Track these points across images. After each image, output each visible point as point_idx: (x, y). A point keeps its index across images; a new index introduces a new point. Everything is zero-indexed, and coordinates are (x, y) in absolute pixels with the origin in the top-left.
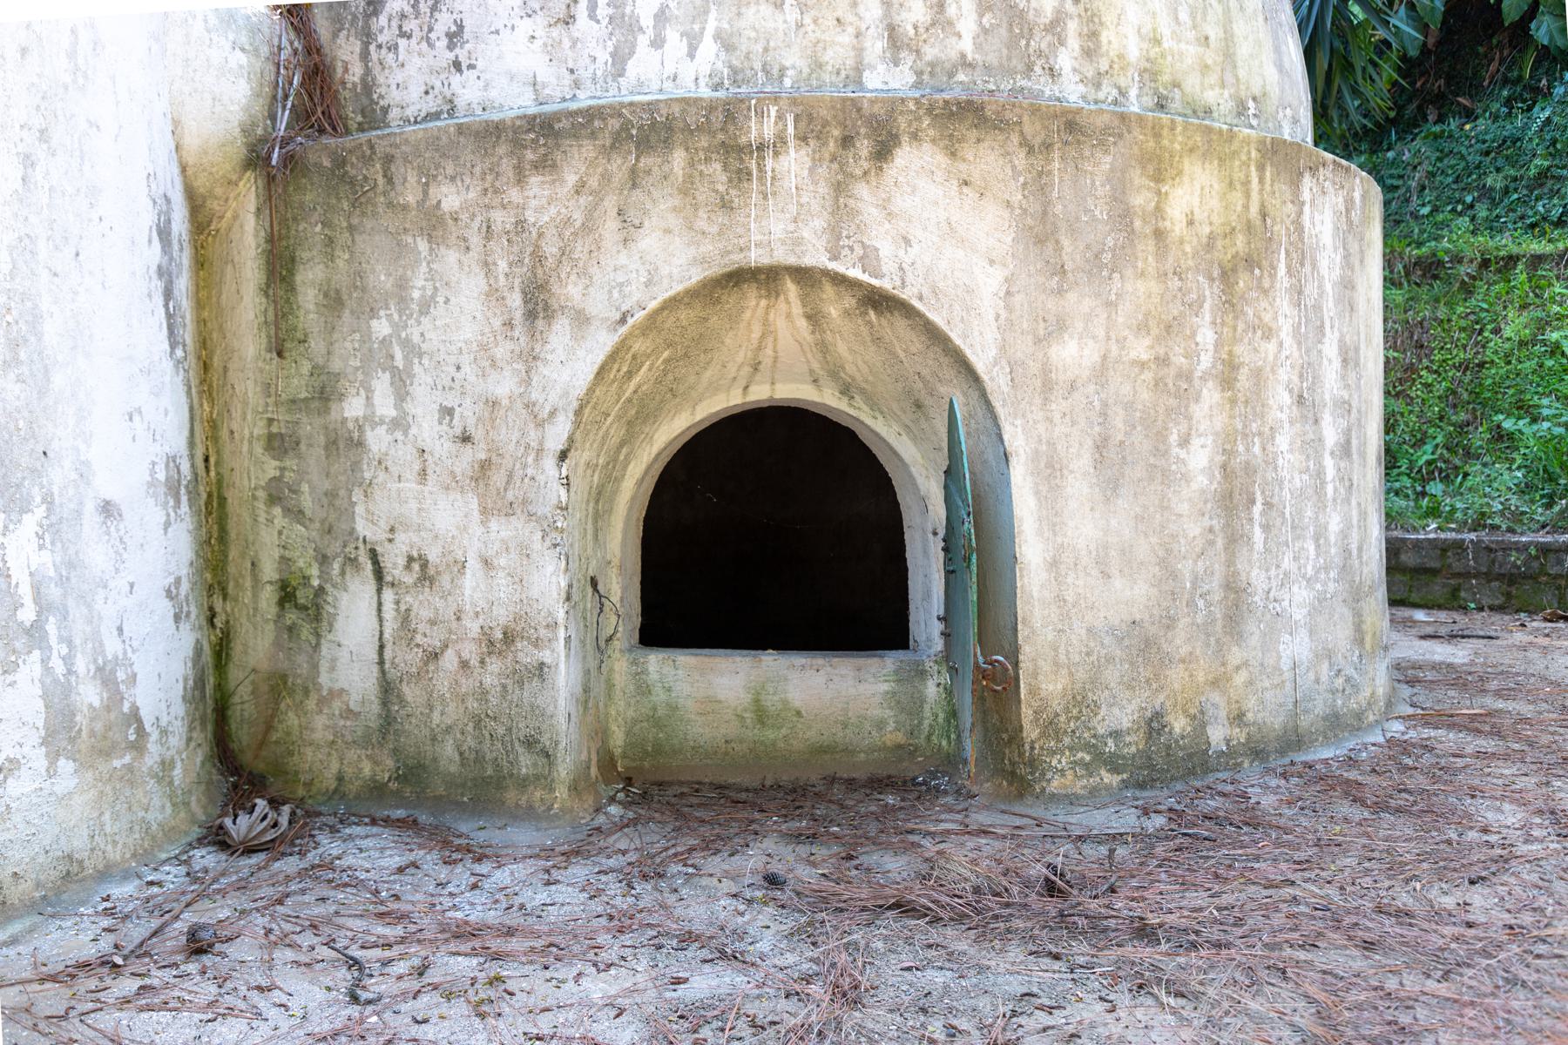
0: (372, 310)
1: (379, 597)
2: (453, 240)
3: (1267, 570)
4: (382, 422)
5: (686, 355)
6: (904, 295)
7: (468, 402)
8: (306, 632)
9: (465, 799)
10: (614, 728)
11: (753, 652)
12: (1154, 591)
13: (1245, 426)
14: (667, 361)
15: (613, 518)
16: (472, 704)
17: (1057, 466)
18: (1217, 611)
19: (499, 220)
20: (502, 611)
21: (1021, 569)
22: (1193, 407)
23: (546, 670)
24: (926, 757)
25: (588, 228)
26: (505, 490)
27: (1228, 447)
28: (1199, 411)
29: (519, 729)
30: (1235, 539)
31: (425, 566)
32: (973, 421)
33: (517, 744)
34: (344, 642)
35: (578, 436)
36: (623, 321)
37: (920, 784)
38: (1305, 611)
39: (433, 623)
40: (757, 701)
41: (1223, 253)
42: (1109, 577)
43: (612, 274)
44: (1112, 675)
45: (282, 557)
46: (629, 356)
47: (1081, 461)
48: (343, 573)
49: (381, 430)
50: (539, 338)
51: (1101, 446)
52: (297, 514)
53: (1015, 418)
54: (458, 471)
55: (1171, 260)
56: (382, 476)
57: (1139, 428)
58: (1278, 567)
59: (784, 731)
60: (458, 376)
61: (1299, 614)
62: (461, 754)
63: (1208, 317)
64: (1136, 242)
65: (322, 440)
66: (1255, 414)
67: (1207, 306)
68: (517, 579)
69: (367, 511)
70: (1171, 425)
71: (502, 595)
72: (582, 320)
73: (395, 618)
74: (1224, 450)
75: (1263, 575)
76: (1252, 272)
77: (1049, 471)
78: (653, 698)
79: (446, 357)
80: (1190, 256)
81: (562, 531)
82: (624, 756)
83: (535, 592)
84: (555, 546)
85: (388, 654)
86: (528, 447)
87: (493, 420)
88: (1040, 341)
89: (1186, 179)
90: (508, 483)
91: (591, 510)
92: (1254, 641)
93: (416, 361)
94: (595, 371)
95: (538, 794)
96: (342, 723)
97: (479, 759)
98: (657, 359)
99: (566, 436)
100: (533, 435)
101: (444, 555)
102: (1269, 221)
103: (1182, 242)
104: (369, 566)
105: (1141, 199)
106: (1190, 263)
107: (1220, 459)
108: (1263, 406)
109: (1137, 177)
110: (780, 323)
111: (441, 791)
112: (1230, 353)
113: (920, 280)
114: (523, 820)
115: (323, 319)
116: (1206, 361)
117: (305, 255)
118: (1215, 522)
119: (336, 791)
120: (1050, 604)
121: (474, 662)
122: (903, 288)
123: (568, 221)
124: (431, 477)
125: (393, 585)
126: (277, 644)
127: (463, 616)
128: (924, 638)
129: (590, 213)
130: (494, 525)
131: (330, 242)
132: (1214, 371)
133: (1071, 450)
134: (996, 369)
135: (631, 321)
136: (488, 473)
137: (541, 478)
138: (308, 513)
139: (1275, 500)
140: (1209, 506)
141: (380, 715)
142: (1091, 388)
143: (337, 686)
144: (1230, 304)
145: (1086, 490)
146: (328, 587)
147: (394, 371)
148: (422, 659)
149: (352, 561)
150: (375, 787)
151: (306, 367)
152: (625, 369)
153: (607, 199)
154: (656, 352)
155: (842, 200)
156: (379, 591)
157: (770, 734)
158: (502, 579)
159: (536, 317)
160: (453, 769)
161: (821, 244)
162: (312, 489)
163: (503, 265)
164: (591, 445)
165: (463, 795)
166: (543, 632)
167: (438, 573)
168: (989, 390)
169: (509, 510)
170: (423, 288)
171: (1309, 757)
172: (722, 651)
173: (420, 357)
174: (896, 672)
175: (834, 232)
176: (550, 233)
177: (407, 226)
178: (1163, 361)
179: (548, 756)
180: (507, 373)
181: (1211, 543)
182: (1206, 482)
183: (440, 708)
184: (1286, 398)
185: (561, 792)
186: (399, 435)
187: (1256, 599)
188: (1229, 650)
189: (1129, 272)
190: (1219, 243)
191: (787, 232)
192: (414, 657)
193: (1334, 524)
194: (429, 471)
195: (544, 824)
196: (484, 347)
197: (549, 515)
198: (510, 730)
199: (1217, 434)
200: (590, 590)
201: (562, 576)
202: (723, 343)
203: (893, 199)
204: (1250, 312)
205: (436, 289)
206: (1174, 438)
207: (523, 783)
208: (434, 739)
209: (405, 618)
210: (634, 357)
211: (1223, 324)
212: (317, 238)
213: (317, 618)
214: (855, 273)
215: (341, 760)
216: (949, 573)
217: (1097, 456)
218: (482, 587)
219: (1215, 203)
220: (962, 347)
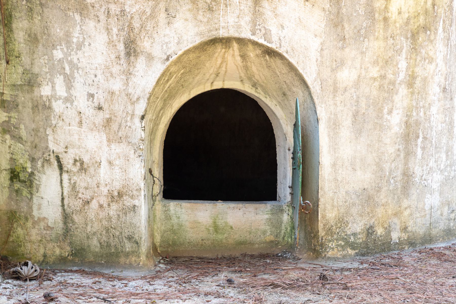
0: (53, 45)
1: (61, 177)
2: (92, 15)
3: (422, 167)
4: (60, 98)
5: (190, 71)
6: (281, 51)
7: (100, 91)
8: (25, 192)
9: (103, 262)
10: (156, 234)
11: (212, 202)
12: (373, 176)
13: (417, 104)
14: (182, 74)
15: (155, 142)
16: (105, 223)
17: (337, 124)
18: (399, 184)
19: (113, 9)
20: (117, 184)
21: (321, 167)
23: (136, 208)
24: (282, 246)
25: (153, 16)
26: (118, 131)
27: (409, 113)
28: (397, 98)
29: (125, 233)
30: (409, 154)
31: (82, 163)
32: (306, 104)
33: (124, 239)
34: (44, 196)
35: (148, 109)
36: (168, 59)
37: (280, 256)
38: (439, 184)
39: (86, 188)
40: (215, 223)
41: (413, 26)
42: (356, 170)
43: (163, 38)
45: (11, 158)
46: (168, 74)
48: (43, 166)
49: (60, 102)
50: (132, 65)
51: (355, 115)
52: (19, 139)
53: (322, 104)
54: (97, 122)
55: (390, 31)
56: (61, 123)
57: (371, 107)
58: (427, 165)
59: (225, 235)
60: (96, 80)
61: (435, 186)
62: (100, 243)
63: (404, 56)
64: (375, 24)
65: (30, 105)
67: (404, 51)
68: (123, 170)
69: (54, 139)
70: (385, 105)
71: (117, 177)
72: (150, 58)
73: (69, 186)
74: (407, 115)
75: (420, 169)
76: (426, 33)
77: (334, 126)
78: (172, 221)
79: (90, 71)
80: (398, 28)
81: (142, 150)
82: (160, 246)
83: (131, 176)
84: (140, 156)
85: (66, 202)
86: (127, 113)
87: (112, 101)
88: (333, 70)
90: (119, 128)
91: (149, 139)
93: (76, 71)
94: (156, 81)
95: (133, 259)
96: (45, 232)
97: (109, 245)
98: (179, 73)
99: (144, 109)
100: (130, 108)
101: (91, 159)
102: (436, 7)
104: (56, 163)
107: (405, 119)
110: (229, 58)
111: (92, 259)
113: (287, 44)
114: (129, 269)
115: (28, 47)
116: (402, 76)
117: (18, 15)
118: (400, 147)
119: (43, 261)
120: (331, 181)
121: (105, 205)
122: (280, 48)
123: (144, 12)
124: (84, 125)
125: (67, 172)
126: (10, 198)
127: (100, 186)
128: (283, 195)
129: (153, 9)
130: (113, 146)
131: (31, 10)
132: (405, 80)
133: (343, 117)
134: (316, 82)
135: (171, 60)
136: (110, 124)
137: (133, 127)
138: (24, 138)
139: (428, 136)
140: (399, 139)
141: (63, 228)
142: (353, 90)
143: (42, 216)
144: (415, 49)
146: (36, 172)
147: (65, 75)
148: (82, 204)
149: (48, 161)
150: (62, 259)
151: (20, 70)
152: (166, 79)
153: (161, 3)
154: (178, 71)
155: (257, 8)
156: (61, 174)
157: (220, 237)
158: (117, 170)
159: (130, 56)
160: (97, 250)
161: (248, 28)
162: (26, 128)
163: (115, 30)
164: (152, 111)
165: (101, 260)
166: (135, 193)
167: (88, 167)
168: (312, 92)
169: (120, 140)
170: (78, 37)
171: (432, 246)
172: (199, 201)
173: (78, 69)
174: (271, 210)
175: (254, 23)
176: (136, 17)
177: (70, 7)
178: (383, 77)
179: (137, 243)
180: (118, 80)
181: (399, 156)
183: (90, 225)
184: (437, 90)
185: (143, 258)
186: (68, 105)
187: (416, 179)
189: (372, 38)
190: (412, 22)
191: (235, 22)
192: (78, 204)
194: (84, 122)
195: (138, 270)
196: (107, 67)
197: (137, 143)
198: (121, 233)
200: (149, 174)
201: (143, 169)
202: (205, 66)
203: (277, 8)
204: (423, 51)
205: (84, 38)
206: (385, 111)
207: (127, 255)
208: (88, 238)
209: (74, 187)
210: (170, 74)
212: (23, 7)
213: (31, 186)
214: (261, 41)
215: (45, 248)
216: (294, 169)
217: (354, 119)
218: (108, 173)
220: (303, 73)
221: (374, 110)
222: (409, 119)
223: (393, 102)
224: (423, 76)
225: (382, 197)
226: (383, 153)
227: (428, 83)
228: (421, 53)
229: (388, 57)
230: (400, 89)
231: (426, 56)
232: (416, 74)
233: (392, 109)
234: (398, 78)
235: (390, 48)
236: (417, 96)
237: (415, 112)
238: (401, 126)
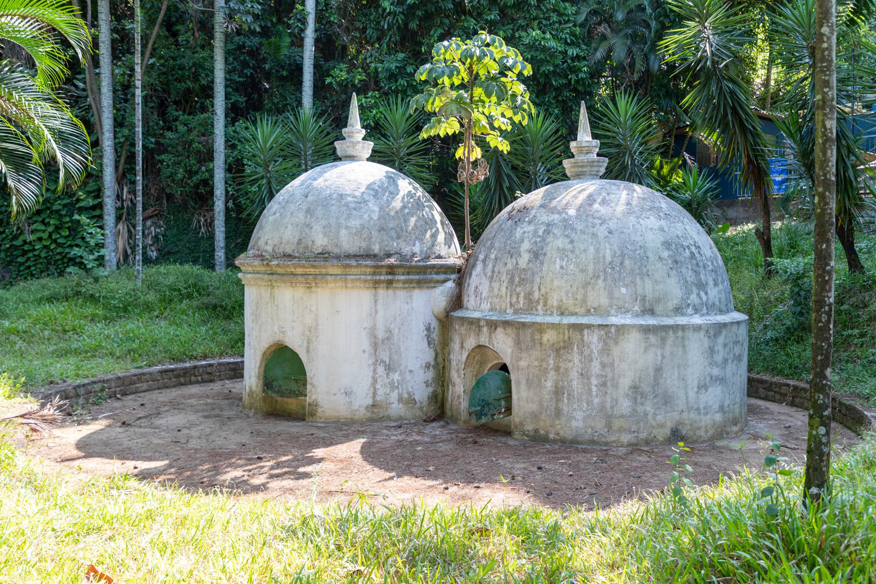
30: (558, 400)
44: (528, 420)
47: (524, 382)
51: (528, 380)
92: (564, 420)
109: (536, 333)
116: (551, 366)
178: (541, 366)
193: (596, 401)
225: (543, 417)
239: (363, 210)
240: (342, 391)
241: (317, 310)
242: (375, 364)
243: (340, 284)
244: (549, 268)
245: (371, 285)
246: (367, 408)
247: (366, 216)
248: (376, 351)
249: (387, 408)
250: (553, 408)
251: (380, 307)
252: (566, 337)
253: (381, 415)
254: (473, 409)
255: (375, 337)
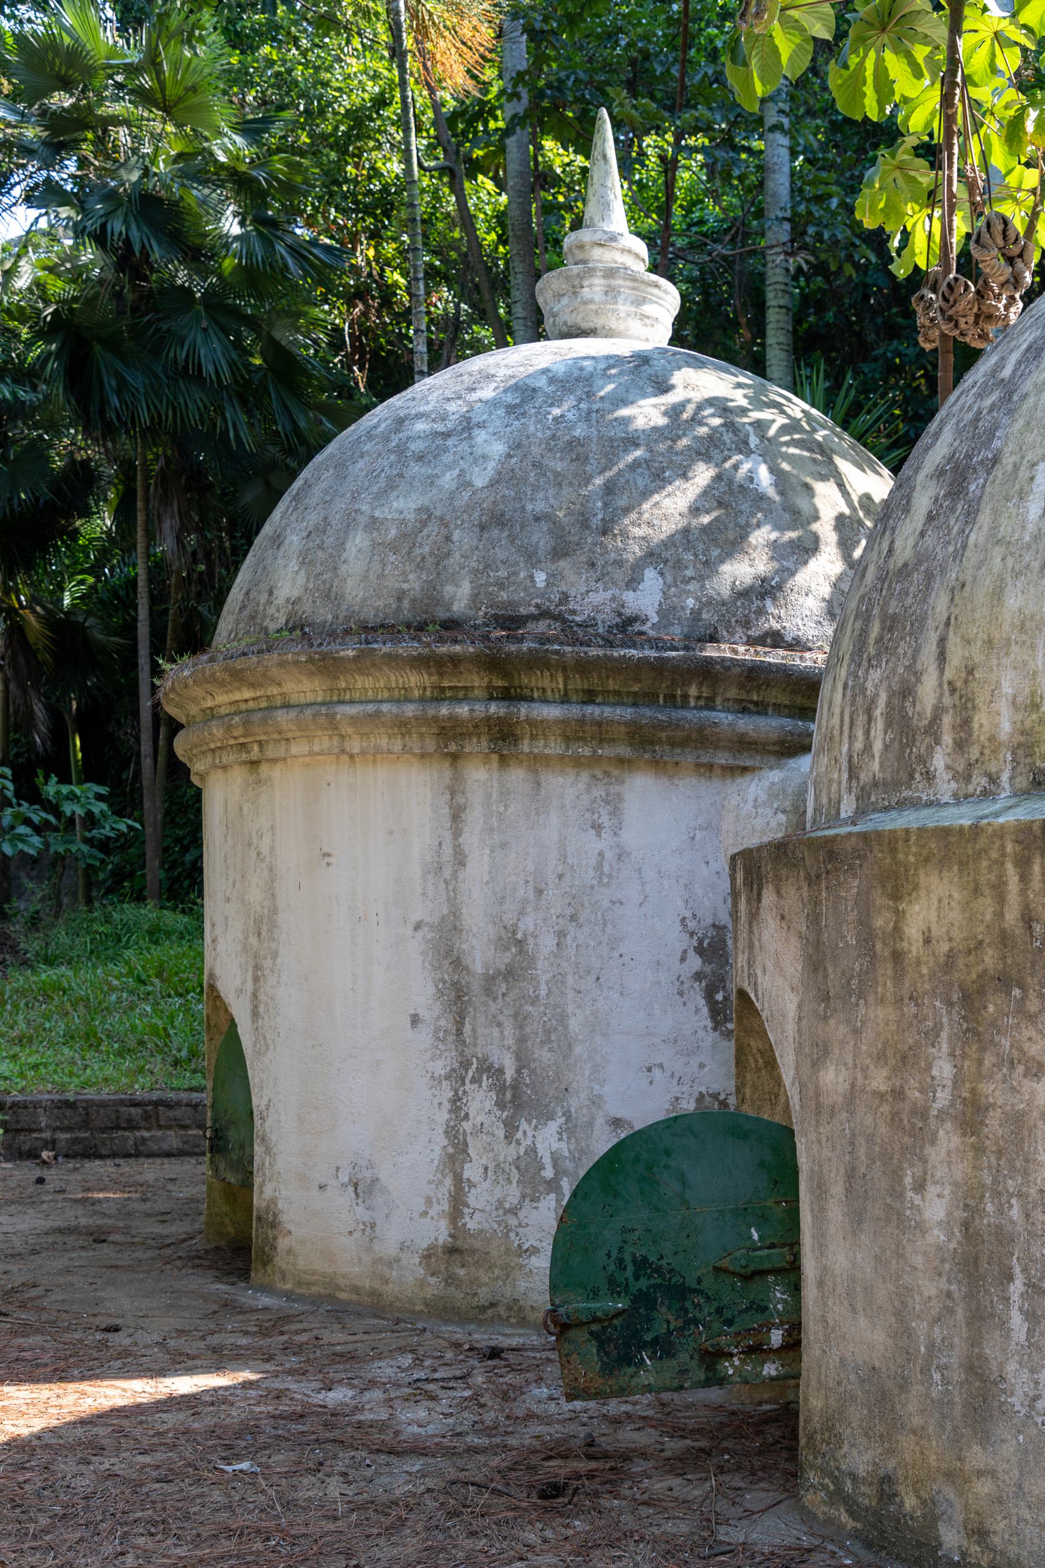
13: (996, 1181)
18: (956, 1393)
22: (929, 1150)
27: (972, 1203)
28: (936, 1154)
44: (856, 1414)
47: (837, 1189)
63: (945, 1048)
66: (1013, 1169)
67: (944, 1035)
74: (966, 1206)
76: (1009, 994)
80: (926, 978)
89: (922, 893)
92: (1008, 1450)
103: (918, 963)
105: (882, 921)
106: (927, 986)
107: (960, 1214)
108: (1027, 1161)
109: (880, 899)
112: (973, 1091)
116: (943, 1098)
132: (951, 1111)
140: (947, 1266)
145: (840, 1218)
182: (943, 1238)
188: (969, 1447)
190: (961, 962)
199: (956, 1184)
204: (1006, 1043)
206: (908, 1180)
211: (964, 1056)
219: (955, 915)
221: (884, 1173)
222: (973, 1218)
223: (924, 1161)
224: (1008, 1108)
226: (909, 1290)
227: (1030, 1130)
228: (995, 1046)
229: (906, 1047)
230: (941, 1132)
231: (1015, 1053)
232: (983, 1100)
233: (925, 1180)
234: (934, 1101)
235: (911, 1024)
236: (993, 1159)
237: (992, 1202)
238: (953, 1233)
239: (447, 458)
240: (344, 1178)
241: (272, 848)
242: (457, 1076)
243: (324, 742)
244: (995, 527)
245: (431, 745)
246: (428, 1256)
247: (448, 480)
248: (460, 1024)
249: (508, 1271)
250: (954, 1358)
251: (472, 838)
252: (1012, 916)
253: (484, 1295)
254: (578, 1305)
255: (457, 964)
